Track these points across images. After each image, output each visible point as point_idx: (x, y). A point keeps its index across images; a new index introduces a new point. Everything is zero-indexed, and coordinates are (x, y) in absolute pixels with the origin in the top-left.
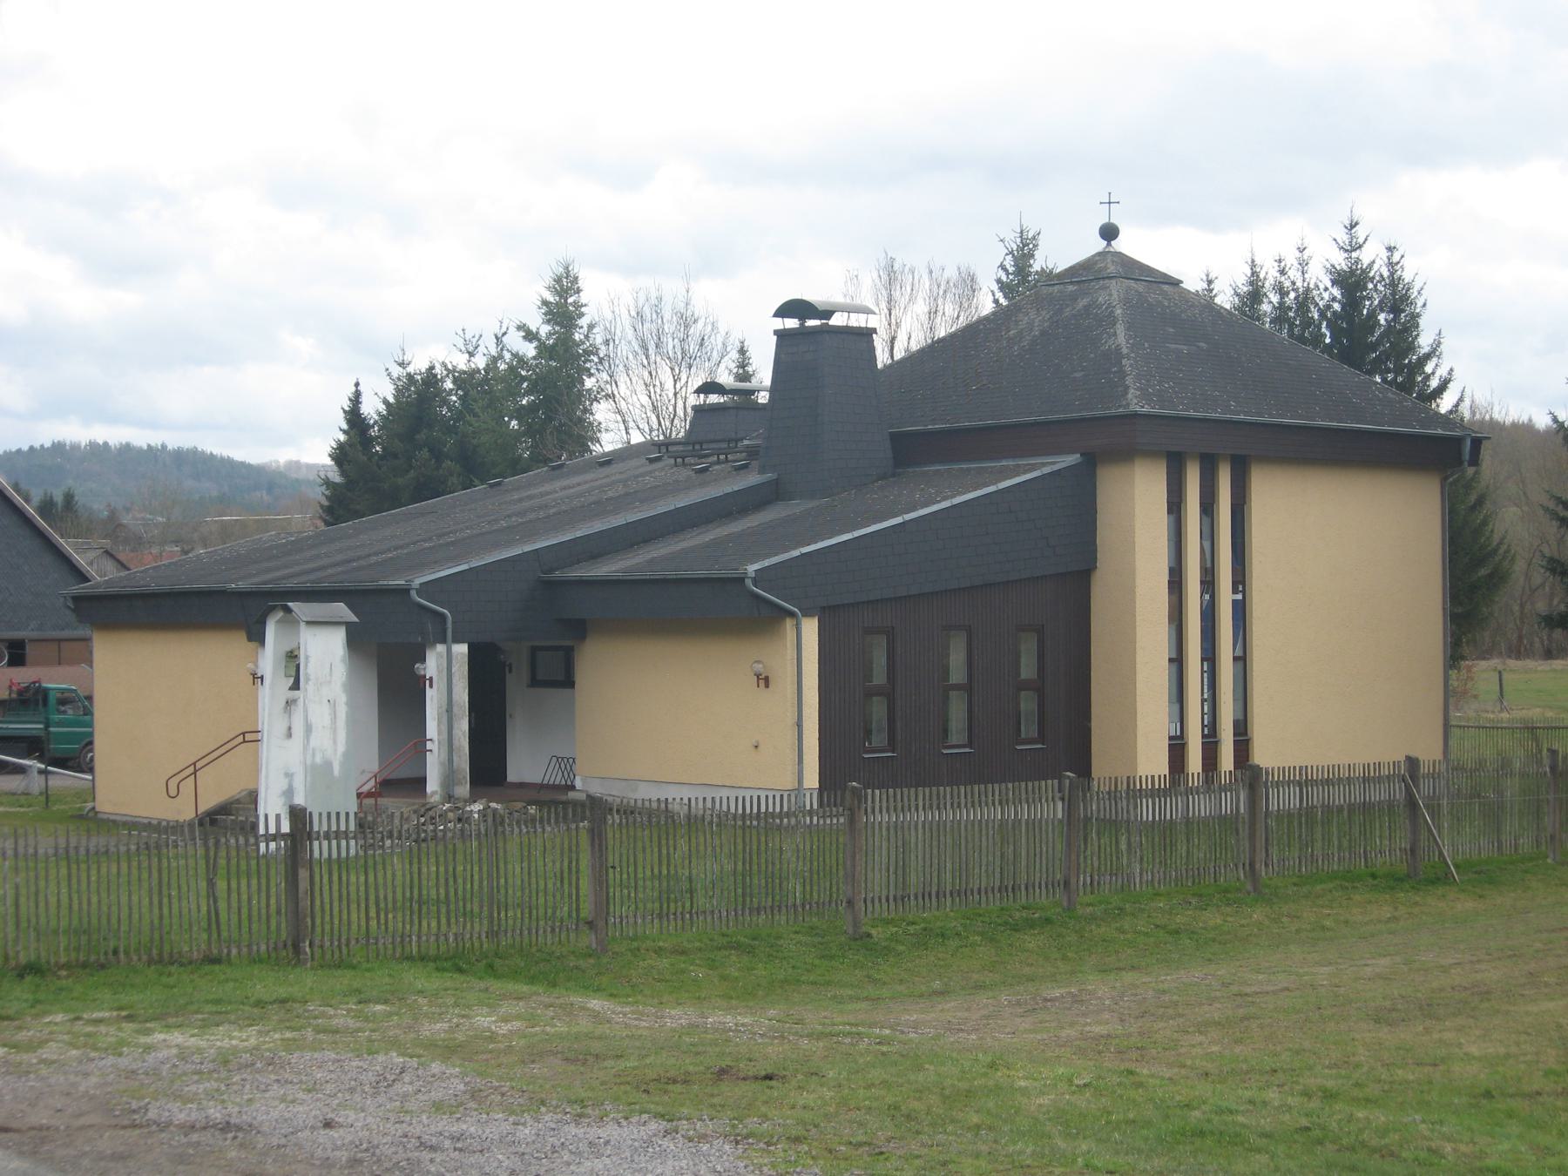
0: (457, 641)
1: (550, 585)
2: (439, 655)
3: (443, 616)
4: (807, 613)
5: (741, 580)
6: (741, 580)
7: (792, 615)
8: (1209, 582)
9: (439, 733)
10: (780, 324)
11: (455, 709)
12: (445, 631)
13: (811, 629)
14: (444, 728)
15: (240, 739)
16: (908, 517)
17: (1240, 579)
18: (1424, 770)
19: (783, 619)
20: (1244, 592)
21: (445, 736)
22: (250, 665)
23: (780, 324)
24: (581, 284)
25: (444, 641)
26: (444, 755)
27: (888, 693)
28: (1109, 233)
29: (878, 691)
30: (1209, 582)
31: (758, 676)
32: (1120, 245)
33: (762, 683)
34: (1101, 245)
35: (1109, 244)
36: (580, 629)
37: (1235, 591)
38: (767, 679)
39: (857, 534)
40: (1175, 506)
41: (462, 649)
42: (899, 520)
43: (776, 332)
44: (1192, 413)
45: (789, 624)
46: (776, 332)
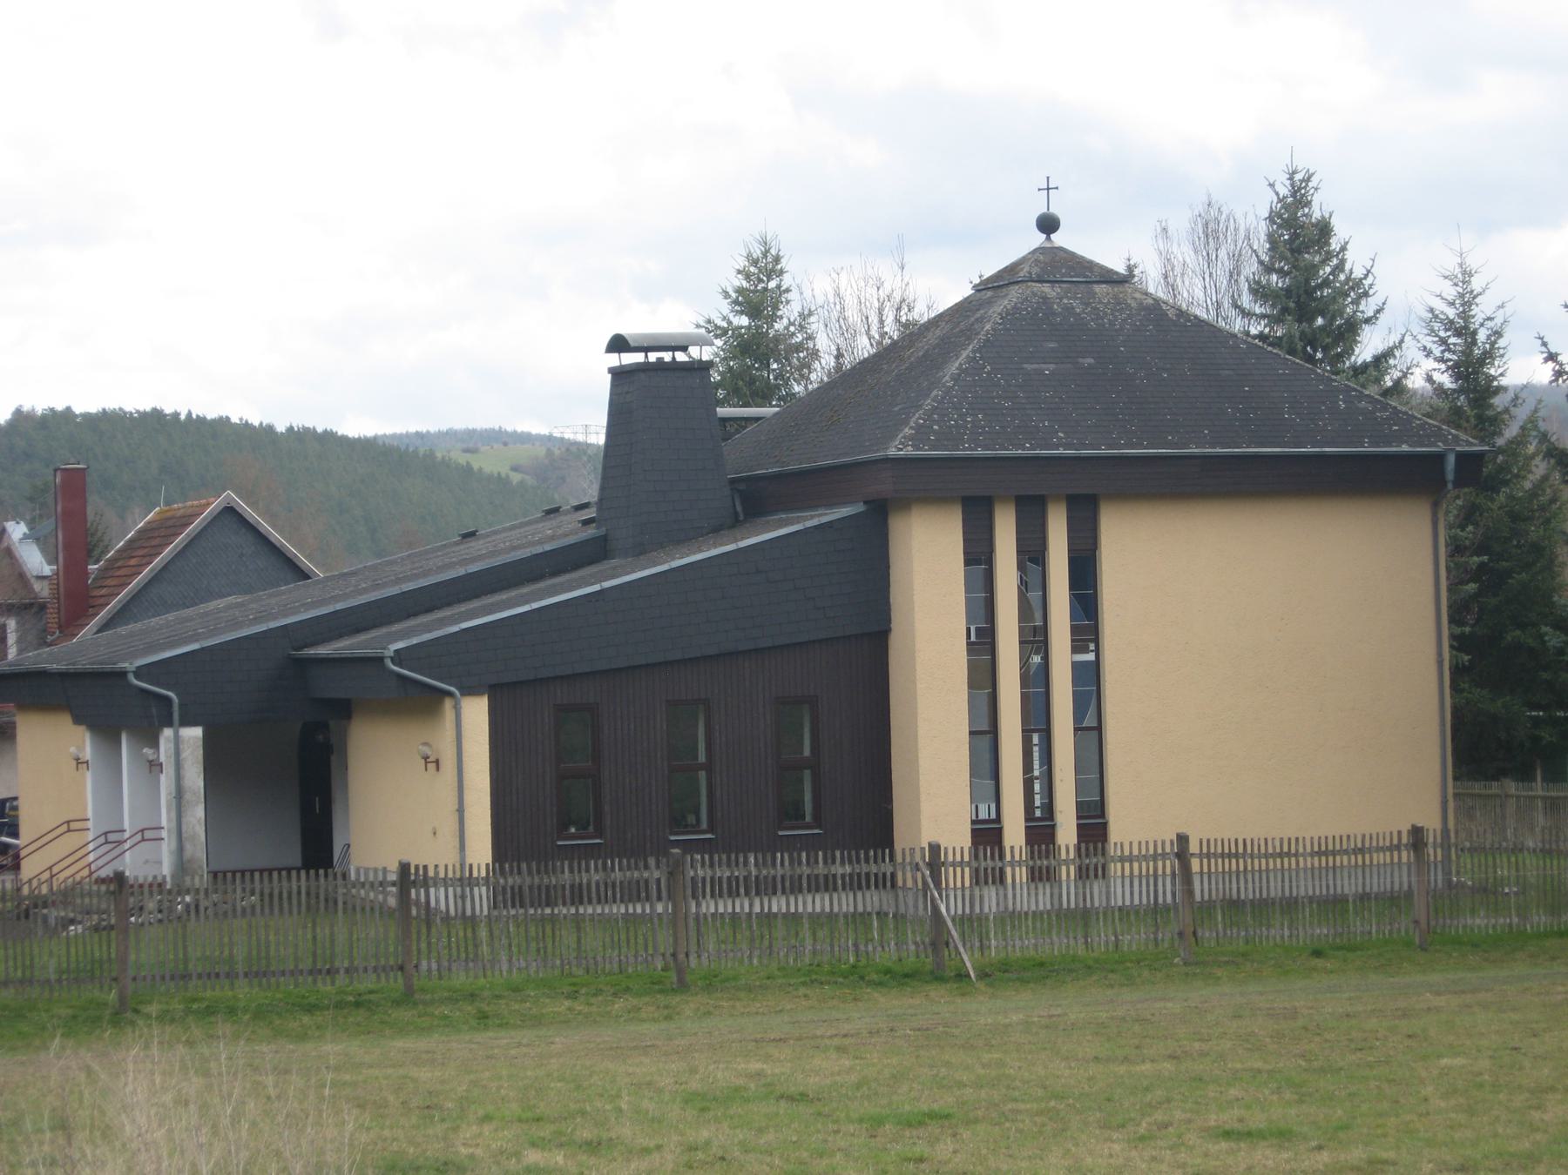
0: (186, 722)
1: (305, 665)
2: (168, 739)
3: (168, 700)
4: (470, 691)
5: (380, 660)
6: (381, 659)
7: (450, 694)
8: (1035, 638)
9: (169, 820)
10: (614, 360)
11: (188, 796)
12: (171, 715)
13: (476, 713)
14: (173, 815)
15: (65, 828)
16: (607, 584)
17: (1087, 628)
18: (1194, 847)
19: (440, 703)
20: (1097, 652)
21: (174, 824)
22: (73, 749)
23: (614, 360)
24: (783, 263)
25: (170, 724)
26: (174, 845)
27: (709, 768)
28: (1048, 224)
29: (702, 767)
30: (1035, 638)
31: (426, 758)
32: (1058, 239)
33: (432, 767)
34: (1039, 239)
35: (1048, 238)
36: (344, 710)
37: (1076, 649)
38: (437, 762)
39: (535, 605)
40: (979, 555)
41: (194, 733)
42: (596, 588)
43: (612, 371)
44: (980, 452)
45: (448, 704)
46: (612, 371)
